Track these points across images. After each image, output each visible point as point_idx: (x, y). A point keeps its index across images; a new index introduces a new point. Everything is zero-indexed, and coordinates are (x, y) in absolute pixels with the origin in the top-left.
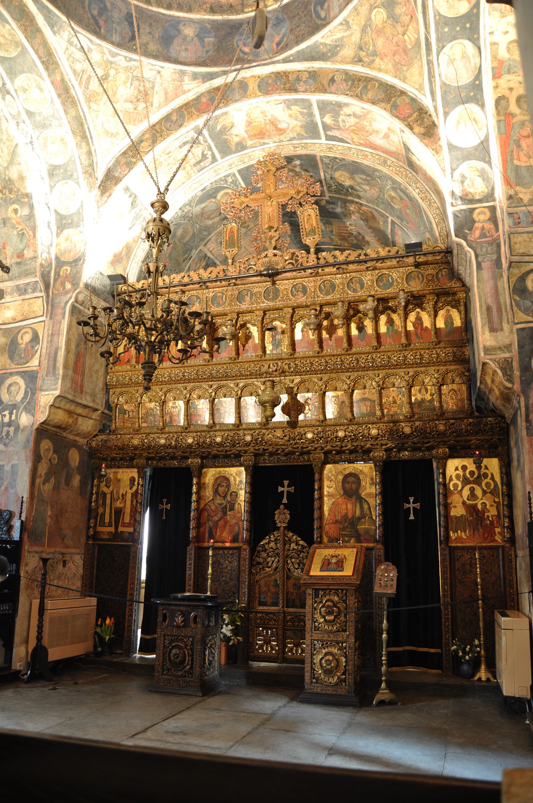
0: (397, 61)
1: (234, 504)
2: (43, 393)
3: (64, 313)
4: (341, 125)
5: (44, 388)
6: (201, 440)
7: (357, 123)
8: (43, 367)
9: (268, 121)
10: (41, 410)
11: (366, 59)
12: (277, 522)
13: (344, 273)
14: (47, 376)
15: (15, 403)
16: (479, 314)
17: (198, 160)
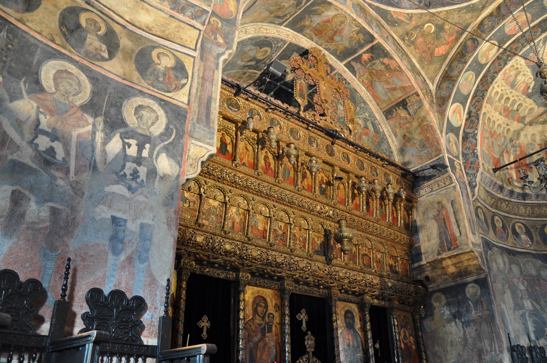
0: (423, 56)
1: (271, 326)
2: (193, 141)
3: (218, 64)
4: (369, 65)
5: (196, 135)
6: (264, 256)
7: (381, 71)
8: (192, 110)
9: (335, 29)
10: (190, 161)
11: (406, 42)
12: (307, 346)
13: (370, 161)
14: (198, 122)
15: (148, 134)
16: (466, 221)
17: (281, 15)
